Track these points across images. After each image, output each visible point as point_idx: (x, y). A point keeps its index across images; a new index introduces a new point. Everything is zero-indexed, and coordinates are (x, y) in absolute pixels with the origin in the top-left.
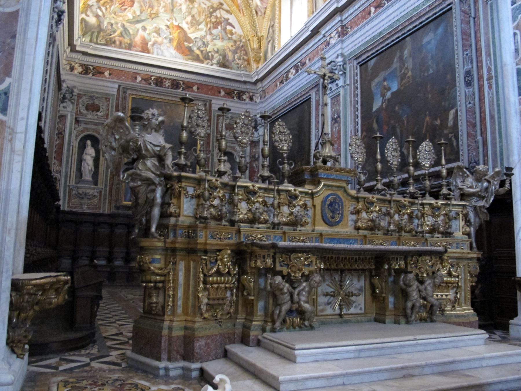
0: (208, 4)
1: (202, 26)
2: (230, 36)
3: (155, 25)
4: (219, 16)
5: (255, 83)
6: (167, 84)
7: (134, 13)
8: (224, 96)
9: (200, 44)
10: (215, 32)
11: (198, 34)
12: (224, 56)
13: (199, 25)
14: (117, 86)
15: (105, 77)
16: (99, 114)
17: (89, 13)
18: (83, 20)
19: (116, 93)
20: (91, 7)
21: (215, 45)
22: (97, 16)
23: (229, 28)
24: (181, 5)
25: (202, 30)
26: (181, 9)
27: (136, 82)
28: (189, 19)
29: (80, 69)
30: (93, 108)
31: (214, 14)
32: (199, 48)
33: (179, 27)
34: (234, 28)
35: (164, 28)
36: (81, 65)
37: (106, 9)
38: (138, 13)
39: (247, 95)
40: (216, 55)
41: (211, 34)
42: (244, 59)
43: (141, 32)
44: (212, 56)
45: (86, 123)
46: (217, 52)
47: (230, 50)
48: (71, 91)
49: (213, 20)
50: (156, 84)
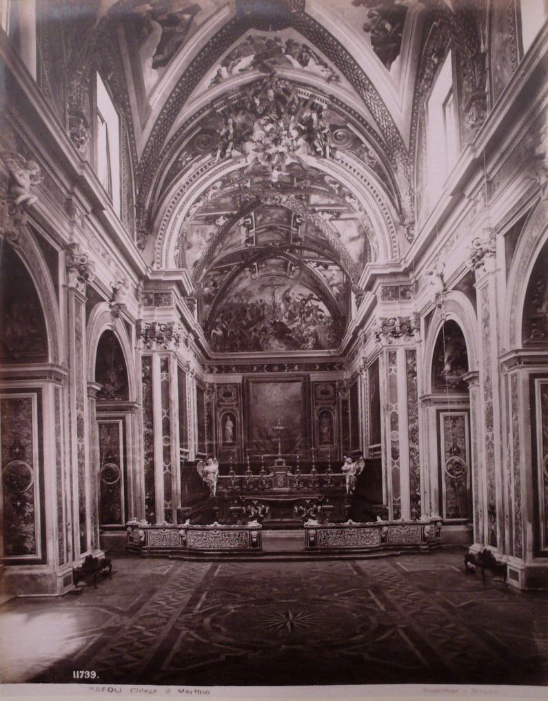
0: (301, 298)
1: (297, 318)
2: (320, 320)
3: (262, 326)
4: (310, 305)
5: (341, 356)
6: (276, 368)
7: (247, 319)
8: (318, 370)
9: (297, 332)
10: (308, 319)
11: (295, 325)
12: (316, 337)
13: (295, 317)
14: (241, 377)
15: (233, 372)
16: (233, 398)
17: (217, 328)
18: (214, 334)
19: (241, 382)
20: (217, 323)
21: (309, 330)
22: (223, 329)
23: (319, 313)
24: (280, 304)
25: (298, 320)
26: (280, 308)
27: (252, 372)
28: (287, 314)
29: (216, 370)
30: (228, 395)
31: (307, 305)
32: (297, 336)
33: (282, 324)
34: (323, 312)
35: (268, 326)
36: (216, 366)
37: (228, 323)
38: (250, 319)
39: (338, 365)
40: (310, 338)
41: (305, 322)
42: (333, 336)
43: (253, 334)
44: (308, 339)
45: (224, 406)
46: (310, 336)
47: (321, 332)
48: (212, 385)
49: (306, 310)
50: (268, 371)
